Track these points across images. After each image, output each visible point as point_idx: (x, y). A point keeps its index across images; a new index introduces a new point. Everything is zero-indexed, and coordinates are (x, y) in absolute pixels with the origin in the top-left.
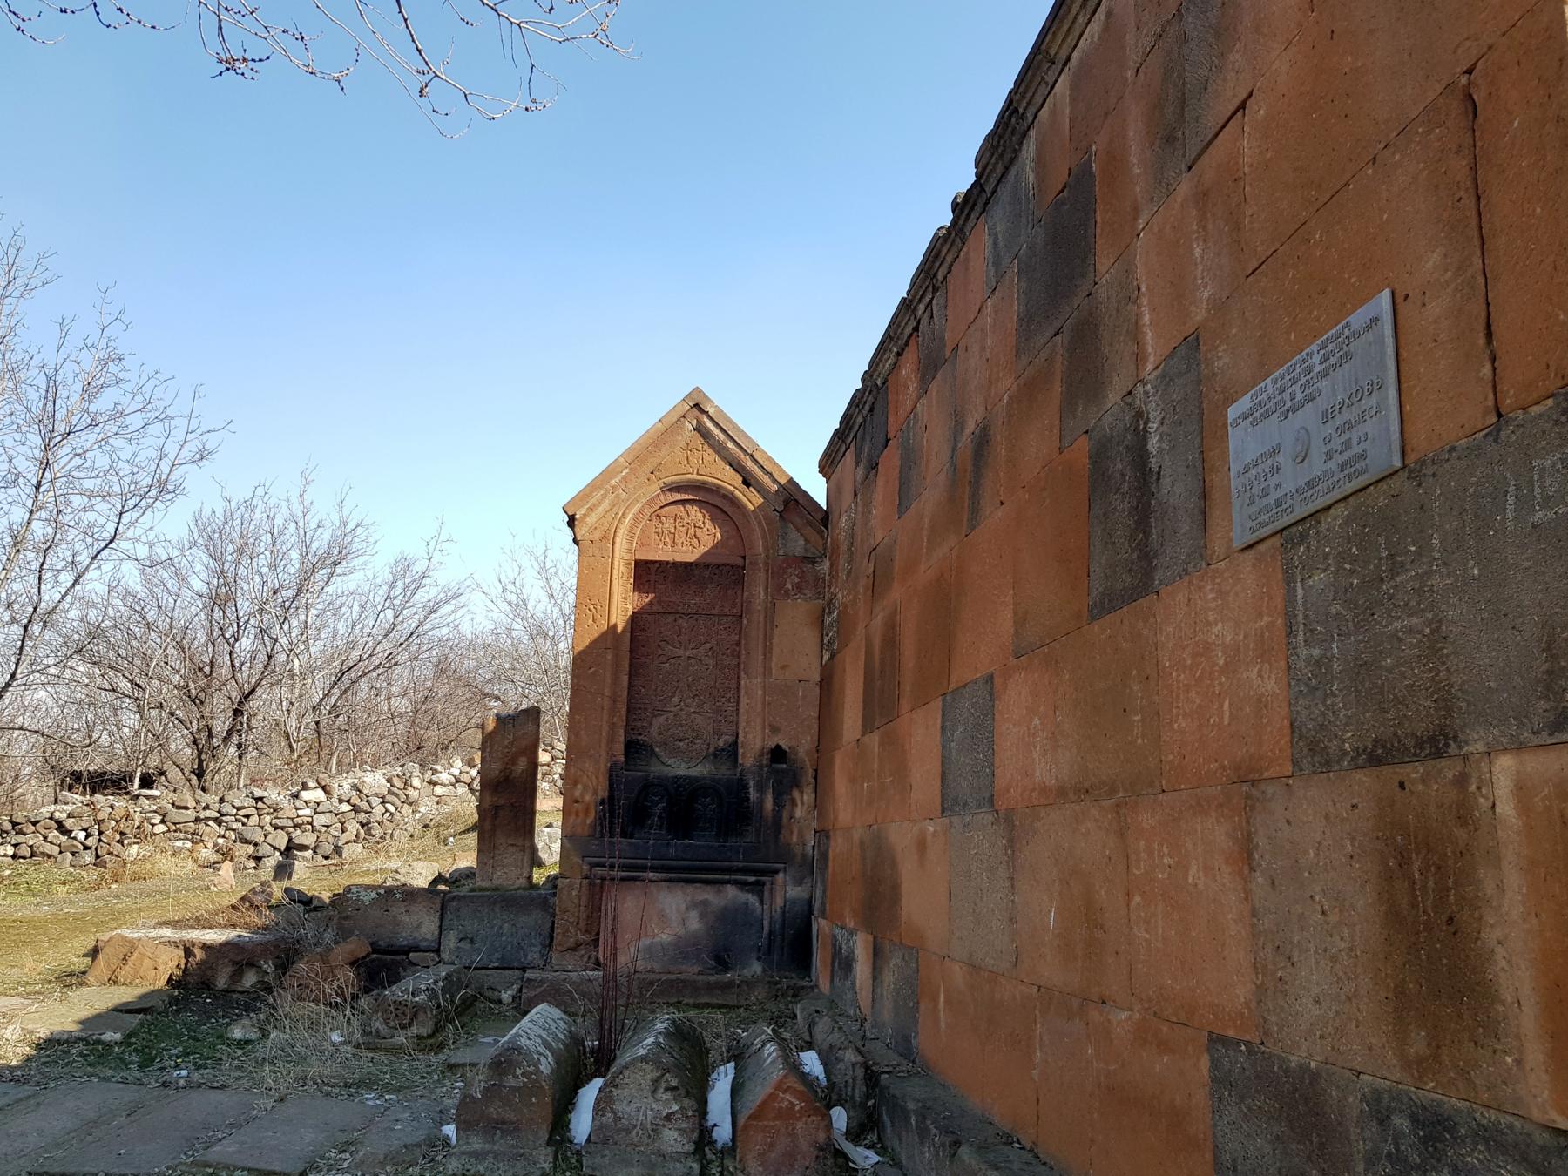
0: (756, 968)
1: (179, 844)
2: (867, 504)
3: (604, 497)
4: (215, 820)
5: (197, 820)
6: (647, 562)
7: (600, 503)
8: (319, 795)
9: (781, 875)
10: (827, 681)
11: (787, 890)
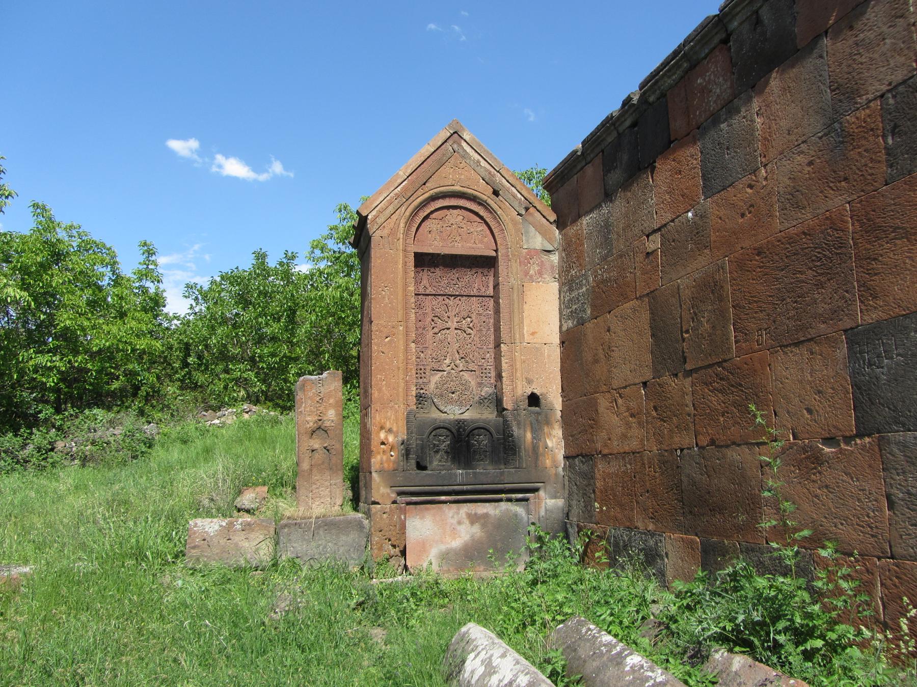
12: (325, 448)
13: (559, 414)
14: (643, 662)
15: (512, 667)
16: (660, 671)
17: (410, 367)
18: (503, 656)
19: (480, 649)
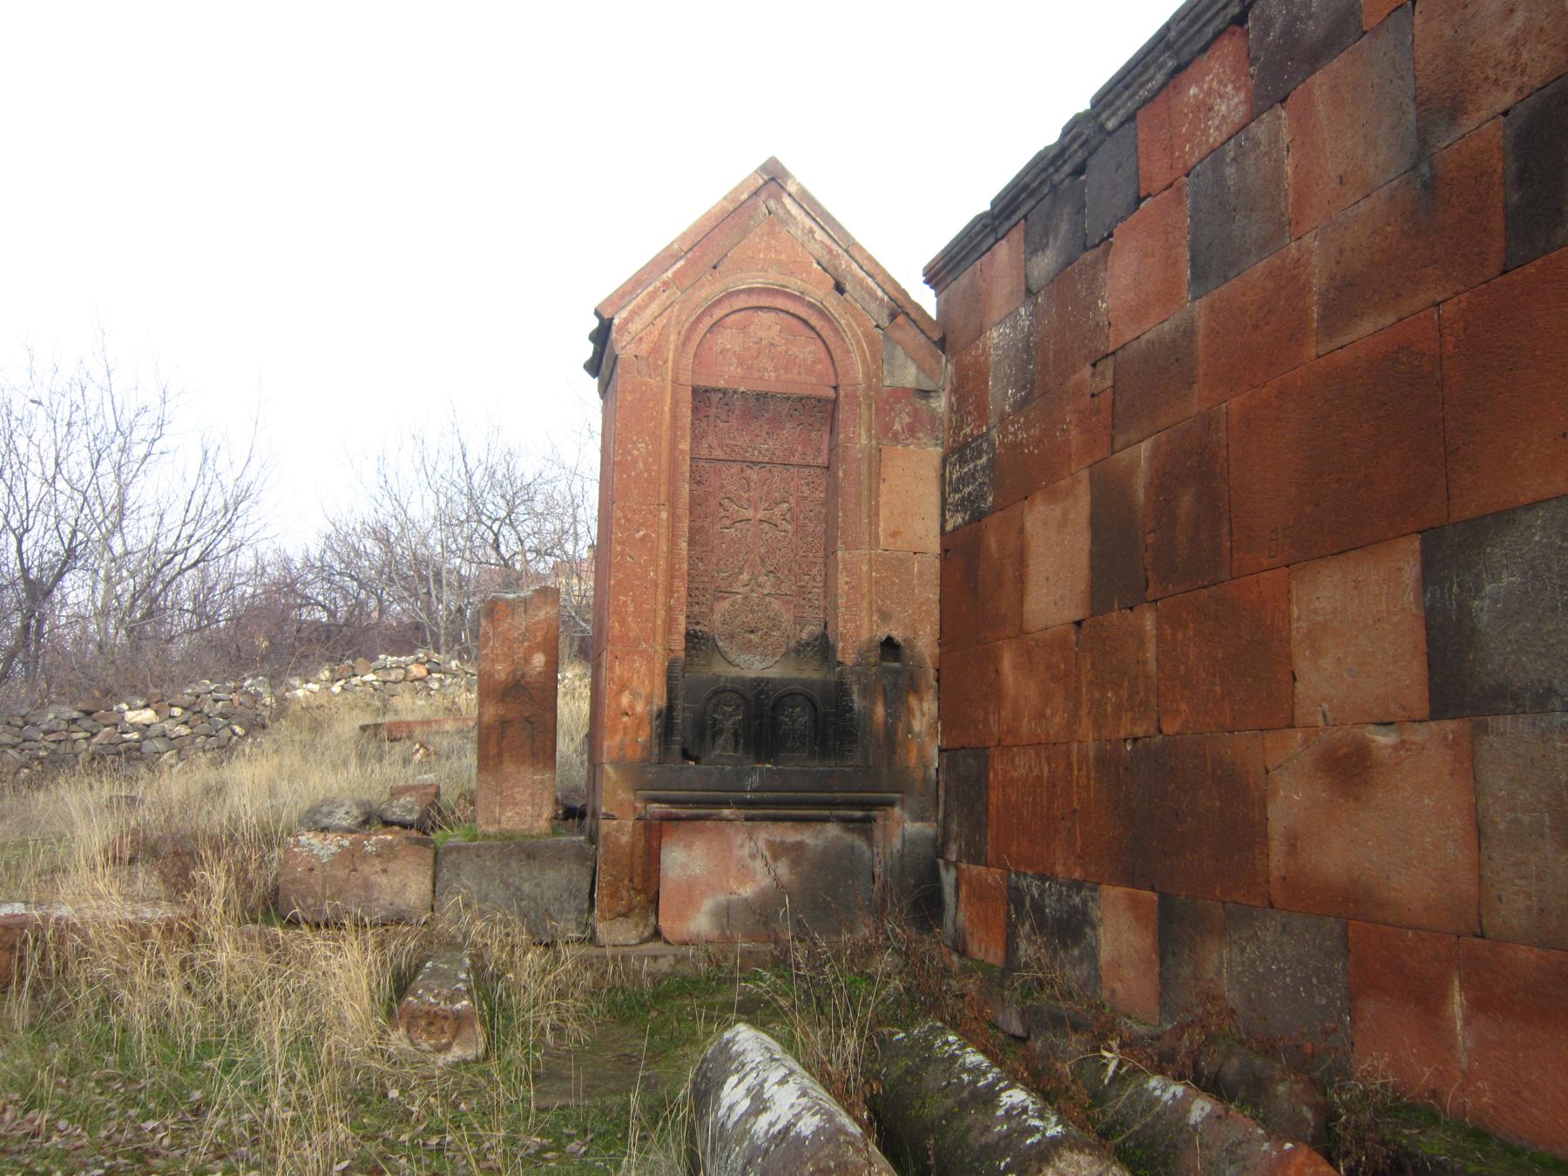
3: (652, 297)
7: (647, 305)
9: (897, 810)
11: (905, 828)
12: (526, 719)
13: (932, 673)
14: (1028, 1102)
15: (793, 1099)
16: (1054, 1119)
17: (677, 582)
18: (783, 1081)
19: (747, 1069)
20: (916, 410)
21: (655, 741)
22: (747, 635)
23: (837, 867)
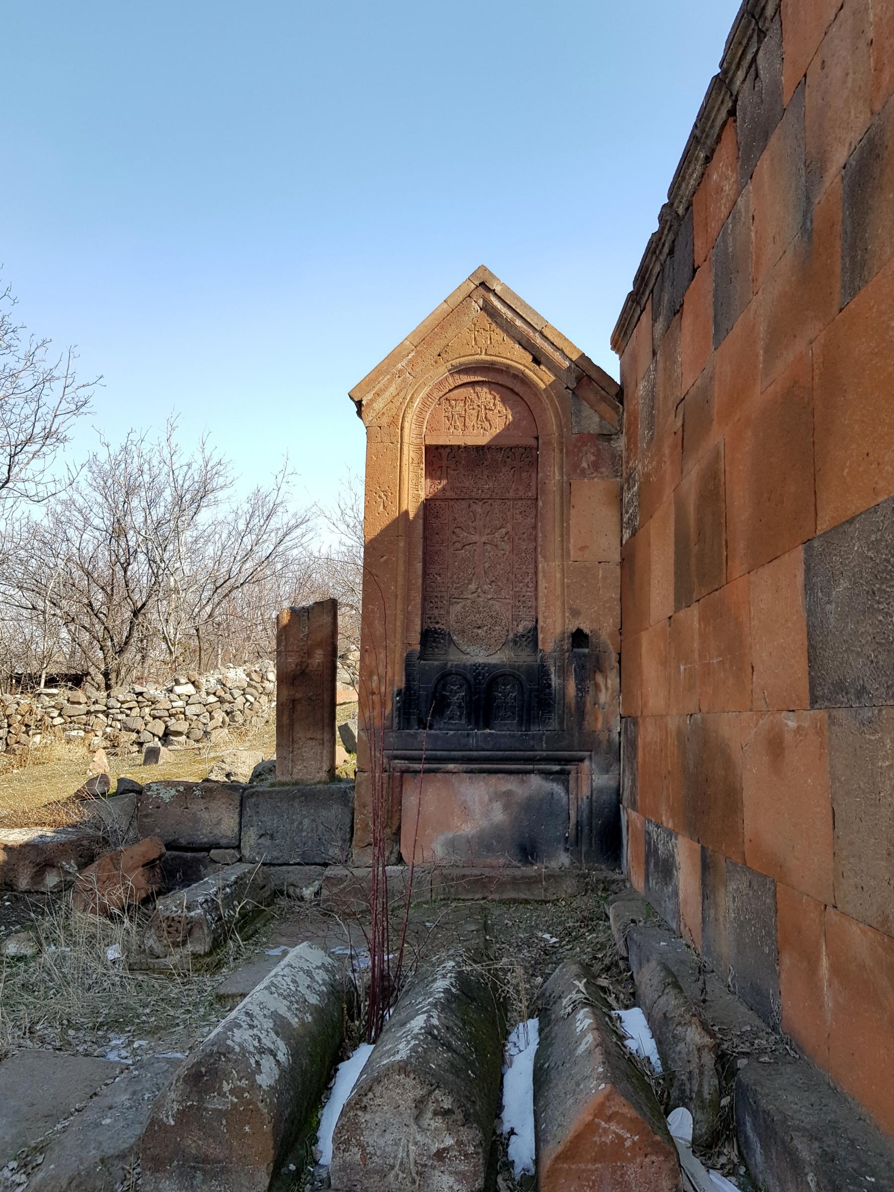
0: (564, 859)
1: (74, 733)
2: (670, 358)
3: (390, 381)
4: (103, 712)
5: (88, 713)
6: (437, 447)
8: (190, 689)
9: (587, 763)
10: (629, 560)
11: (593, 778)
20: (599, 450)
21: (395, 713)
22: (476, 630)
23: (538, 810)
